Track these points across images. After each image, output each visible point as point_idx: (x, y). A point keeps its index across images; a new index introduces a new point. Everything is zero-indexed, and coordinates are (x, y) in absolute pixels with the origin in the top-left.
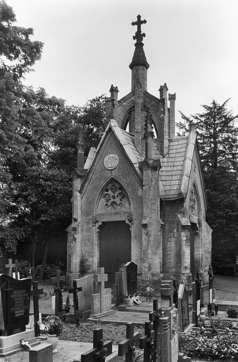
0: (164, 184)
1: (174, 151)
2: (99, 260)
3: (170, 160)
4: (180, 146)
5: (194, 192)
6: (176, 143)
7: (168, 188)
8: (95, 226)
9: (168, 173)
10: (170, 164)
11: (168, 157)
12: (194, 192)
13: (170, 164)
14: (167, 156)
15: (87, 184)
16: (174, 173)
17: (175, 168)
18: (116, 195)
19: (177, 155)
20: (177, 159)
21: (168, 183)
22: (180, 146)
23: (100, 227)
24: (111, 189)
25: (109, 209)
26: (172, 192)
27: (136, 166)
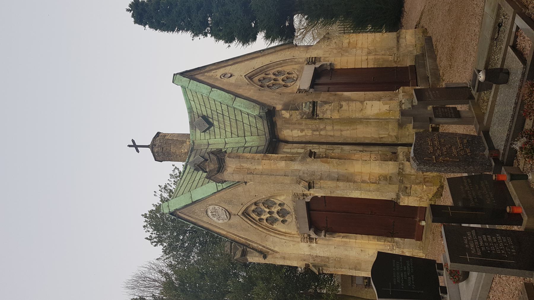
0: (249, 134)
1: (203, 109)
2: (371, 237)
3: (215, 117)
4: (196, 99)
5: (263, 75)
6: (192, 103)
7: (254, 130)
8: (316, 239)
9: (234, 124)
10: (221, 119)
11: (213, 119)
12: (263, 75)
13: (221, 119)
14: (211, 120)
15: (253, 244)
16: (233, 117)
17: (226, 114)
18: (268, 210)
19: (208, 106)
20: (214, 108)
21: (247, 128)
22: (196, 99)
23: (317, 231)
24: (259, 214)
25: (289, 220)
26: (260, 126)
27: (220, 186)
